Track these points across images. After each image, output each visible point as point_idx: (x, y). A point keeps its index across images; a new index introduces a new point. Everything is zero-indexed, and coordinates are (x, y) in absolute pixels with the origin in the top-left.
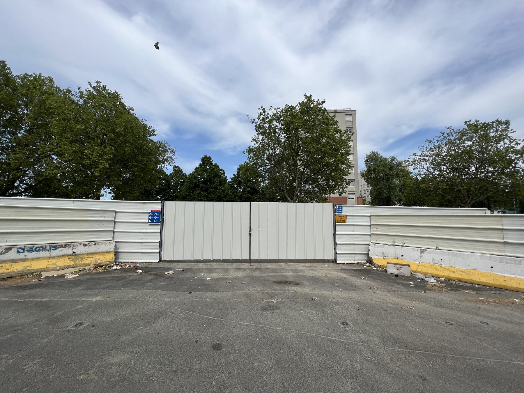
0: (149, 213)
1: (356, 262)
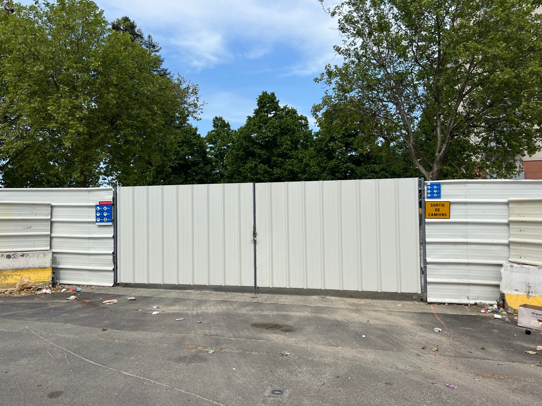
0: (97, 206)
1: (473, 302)
